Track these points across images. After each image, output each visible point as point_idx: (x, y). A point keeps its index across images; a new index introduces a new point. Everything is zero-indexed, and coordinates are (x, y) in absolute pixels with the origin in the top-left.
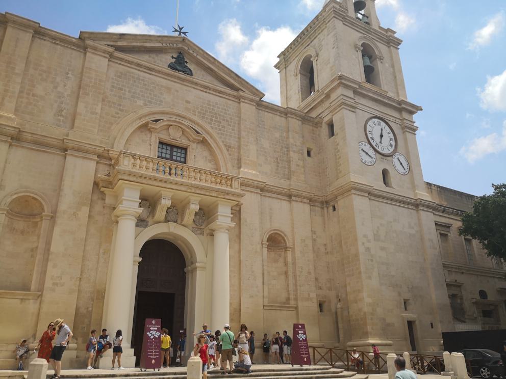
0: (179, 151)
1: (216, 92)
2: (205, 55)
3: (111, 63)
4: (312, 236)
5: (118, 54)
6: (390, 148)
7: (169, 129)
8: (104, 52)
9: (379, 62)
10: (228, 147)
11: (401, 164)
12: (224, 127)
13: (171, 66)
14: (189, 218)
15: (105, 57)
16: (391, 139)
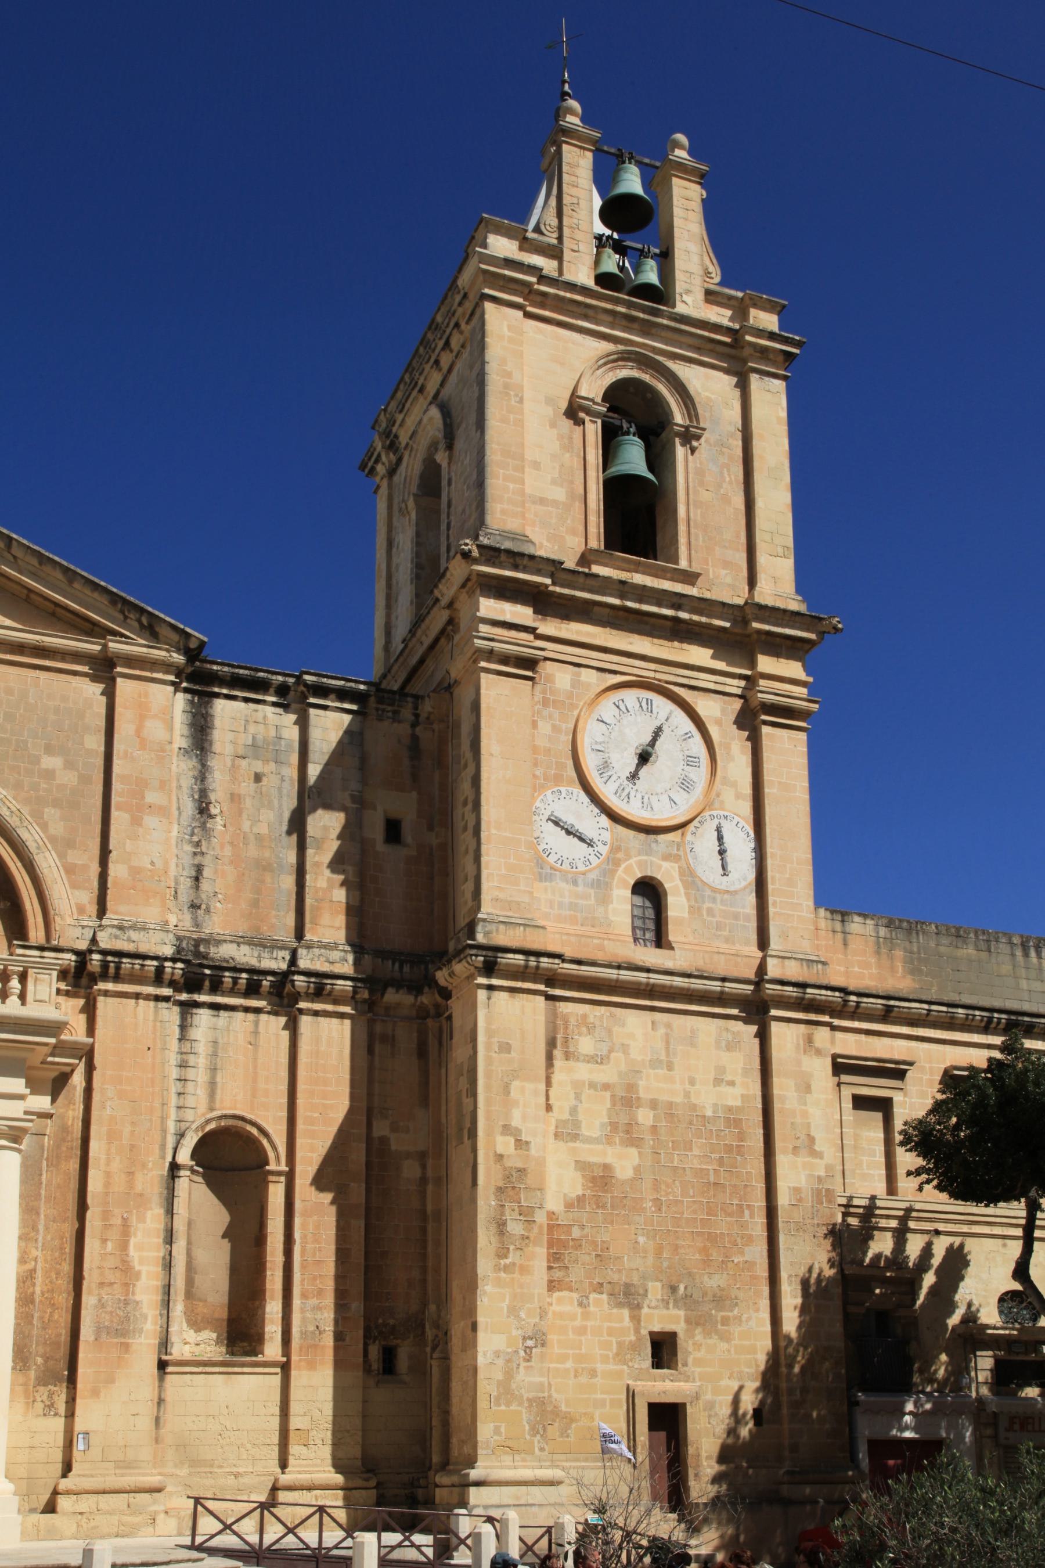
1: (22, 654)
6: (680, 796)
9: (680, 451)
10: (63, 845)
11: (722, 852)
16: (691, 761)
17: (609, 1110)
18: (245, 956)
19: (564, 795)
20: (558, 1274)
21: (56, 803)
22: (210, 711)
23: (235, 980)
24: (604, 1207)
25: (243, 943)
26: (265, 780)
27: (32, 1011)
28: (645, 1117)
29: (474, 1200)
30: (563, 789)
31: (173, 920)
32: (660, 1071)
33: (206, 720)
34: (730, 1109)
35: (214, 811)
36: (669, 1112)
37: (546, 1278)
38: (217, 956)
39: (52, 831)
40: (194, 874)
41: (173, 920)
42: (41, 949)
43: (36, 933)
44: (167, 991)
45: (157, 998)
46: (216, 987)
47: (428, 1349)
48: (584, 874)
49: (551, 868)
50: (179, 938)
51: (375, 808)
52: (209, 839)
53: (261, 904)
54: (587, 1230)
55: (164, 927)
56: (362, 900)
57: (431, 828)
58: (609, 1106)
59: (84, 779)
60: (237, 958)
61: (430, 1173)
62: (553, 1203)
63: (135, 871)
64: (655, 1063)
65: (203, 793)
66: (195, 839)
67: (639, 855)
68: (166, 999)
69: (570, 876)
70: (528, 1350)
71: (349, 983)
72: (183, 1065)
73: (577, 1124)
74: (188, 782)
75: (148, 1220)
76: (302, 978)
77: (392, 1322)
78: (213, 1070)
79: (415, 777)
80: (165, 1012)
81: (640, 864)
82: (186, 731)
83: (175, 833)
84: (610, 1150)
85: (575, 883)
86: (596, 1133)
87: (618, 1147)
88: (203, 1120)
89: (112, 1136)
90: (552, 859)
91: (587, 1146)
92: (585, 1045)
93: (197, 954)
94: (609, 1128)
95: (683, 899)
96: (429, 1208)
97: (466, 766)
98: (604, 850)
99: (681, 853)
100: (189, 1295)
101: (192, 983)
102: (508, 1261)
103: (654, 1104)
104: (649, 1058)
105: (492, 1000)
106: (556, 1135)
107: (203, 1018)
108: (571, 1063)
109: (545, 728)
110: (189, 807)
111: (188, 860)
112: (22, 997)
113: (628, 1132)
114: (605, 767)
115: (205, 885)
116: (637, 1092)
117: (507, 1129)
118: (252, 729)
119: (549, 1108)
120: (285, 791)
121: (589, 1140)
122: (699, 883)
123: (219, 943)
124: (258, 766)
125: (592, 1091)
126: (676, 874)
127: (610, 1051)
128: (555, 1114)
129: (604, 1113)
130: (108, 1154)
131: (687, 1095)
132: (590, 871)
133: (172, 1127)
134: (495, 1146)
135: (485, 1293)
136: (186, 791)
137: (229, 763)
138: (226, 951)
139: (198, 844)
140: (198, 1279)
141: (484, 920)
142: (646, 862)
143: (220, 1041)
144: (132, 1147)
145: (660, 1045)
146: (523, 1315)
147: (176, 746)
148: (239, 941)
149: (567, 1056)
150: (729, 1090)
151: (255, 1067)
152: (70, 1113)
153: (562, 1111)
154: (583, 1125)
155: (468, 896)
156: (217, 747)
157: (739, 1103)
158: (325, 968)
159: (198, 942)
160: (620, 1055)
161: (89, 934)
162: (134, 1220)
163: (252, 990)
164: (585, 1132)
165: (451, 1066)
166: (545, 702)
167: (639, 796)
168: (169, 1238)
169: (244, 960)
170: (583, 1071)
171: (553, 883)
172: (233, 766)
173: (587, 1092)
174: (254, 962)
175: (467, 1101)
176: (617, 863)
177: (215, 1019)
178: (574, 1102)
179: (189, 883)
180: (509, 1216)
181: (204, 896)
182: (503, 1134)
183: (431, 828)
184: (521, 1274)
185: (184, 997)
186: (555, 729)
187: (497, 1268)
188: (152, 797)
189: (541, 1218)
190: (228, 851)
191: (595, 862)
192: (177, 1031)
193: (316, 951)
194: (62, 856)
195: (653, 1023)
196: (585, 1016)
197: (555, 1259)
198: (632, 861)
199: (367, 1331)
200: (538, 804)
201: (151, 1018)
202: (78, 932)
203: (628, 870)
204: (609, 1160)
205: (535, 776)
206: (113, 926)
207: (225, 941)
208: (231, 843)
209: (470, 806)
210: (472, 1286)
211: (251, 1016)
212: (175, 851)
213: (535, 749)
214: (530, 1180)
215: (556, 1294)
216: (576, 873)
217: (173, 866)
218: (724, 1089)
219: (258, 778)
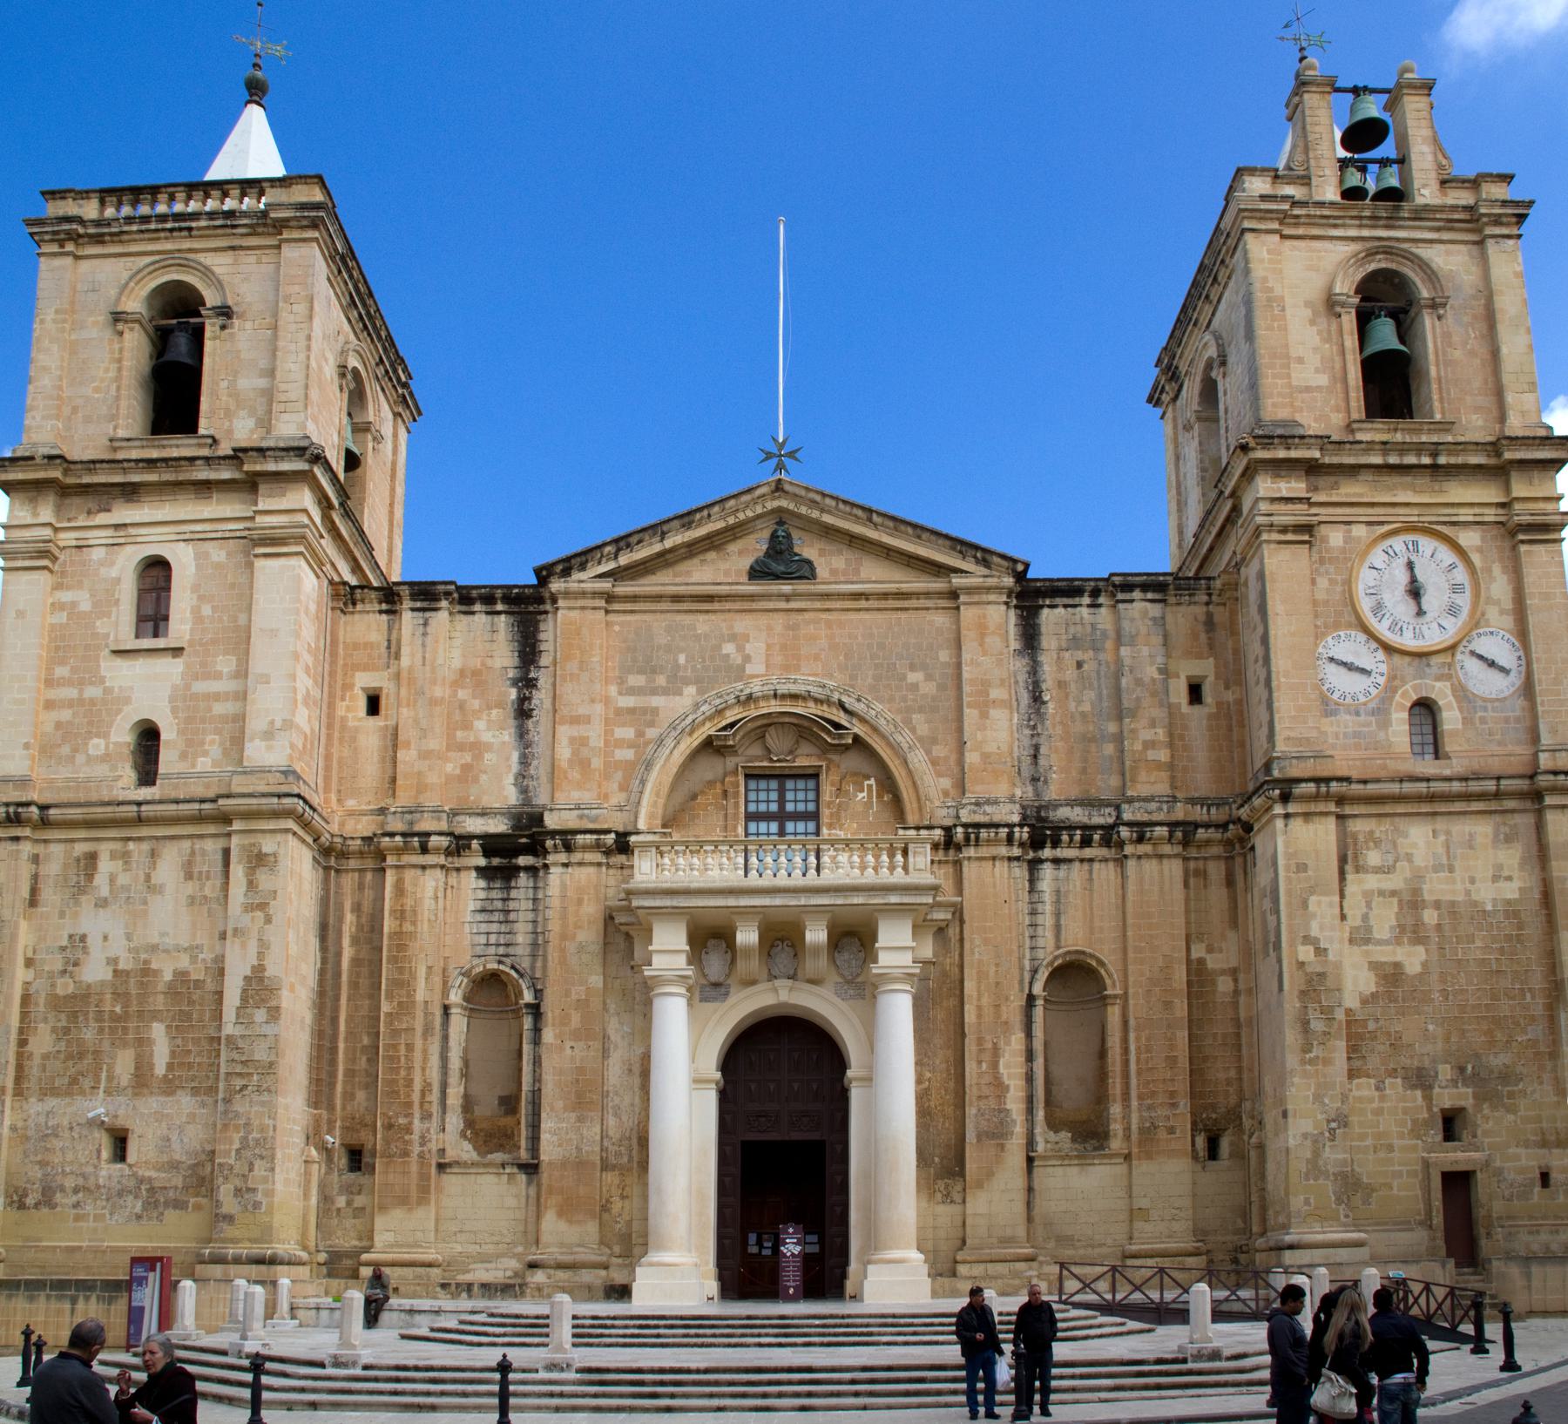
0: (801, 784)
2: (841, 506)
3: (612, 617)
4: (1188, 950)
7: (764, 737)
8: (596, 594)
10: (928, 743)
12: (914, 687)
13: (757, 573)
14: (817, 964)
15: (594, 608)
18: (1077, 815)
20: (1357, 1064)
21: (921, 710)
23: (1071, 837)
24: (1396, 1001)
26: (1086, 667)
27: (914, 878)
29: (1280, 1004)
31: (1018, 793)
34: (1509, 902)
35: (1046, 698)
36: (1451, 910)
37: (1346, 1067)
38: (1055, 819)
39: (919, 732)
40: (1032, 752)
41: (1018, 793)
42: (918, 828)
43: (912, 819)
44: (1016, 852)
45: (1010, 859)
46: (1056, 843)
47: (1246, 1138)
49: (1337, 704)
50: (1023, 807)
51: (1178, 677)
52: (1043, 724)
53: (1089, 771)
54: (1381, 1023)
55: (1012, 800)
56: (1172, 756)
57: (1227, 687)
58: (1396, 910)
59: (942, 687)
61: (1241, 986)
62: (1351, 1001)
63: (985, 757)
66: (1032, 723)
68: (1018, 859)
70: (1332, 1131)
71: (1165, 828)
72: (1033, 913)
74: (1022, 677)
75: (1013, 1043)
76: (1125, 828)
77: (1214, 1116)
78: (1057, 915)
79: (1211, 646)
80: (1017, 870)
83: (1015, 721)
88: (1051, 957)
89: (981, 975)
92: (1373, 858)
93: (1040, 819)
96: (1242, 1015)
97: (1255, 629)
100: (1048, 1103)
101: (1036, 843)
102: (1312, 1055)
105: (1289, 827)
106: (1351, 941)
107: (1047, 872)
109: (1323, 583)
110: (1025, 698)
111: (1027, 742)
112: (905, 868)
114: (1378, 608)
115: (1042, 761)
117: (1307, 940)
119: (1343, 917)
120: (1102, 673)
123: (1056, 807)
124: (1080, 655)
128: (1350, 922)
130: (979, 991)
131: (1468, 893)
133: (1027, 964)
134: (1297, 955)
135: (1293, 1084)
137: (1055, 656)
138: (1063, 813)
139: (1034, 727)
140: (1055, 1089)
141: (1278, 758)
144: (997, 984)
146: (1327, 1101)
147: (1012, 648)
148: (1071, 803)
149: (1358, 869)
150: (1508, 884)
151: (1091, 909)
152: (948, 960)
153: (1354, 918)
155: (1264, 739)
157: (1516, 896)
158: (1146, 818)
159: (1039, 808)
161: (952, 812)
162: (1002, 1044)
163: (1086, 842)
165: (1256, 890)
168: (1030, 1056)
169: (1078, 819)
170: (1372, 882)
173: (1376, 900)
174: (1085, 820)
175: (1271, 919)
177: (1056, 872)
178: (1365, 910)
179: (1029, 760)
180: (1312, 1015)
182: (1304, 944)
183: (1227, 687)
184: (1324, 1065)
185: (1031, 855)
187: (1303, 1062)
188: (996, 693)
189: (1340, 1015)
190: (1059, 730)
192: (1027, 884)
193: (1136, 804)
194: (928, 752)
197: (1353, 1050)
199: (1194, 1124)
200: (1320, 650)
202: (944, 812)
205: (1316, 626)
206: (971, 804)
208: (1061, 723)
209: (1261, 662)
210: (1281, 1081)
211: (1086, 866)
212: (1016, 735)
213: (1315, 603)
214: (1329, 983)
215: (1356, 1081)
217: (1016, 749)
218: (1502, 884)
219: (1079, 665)
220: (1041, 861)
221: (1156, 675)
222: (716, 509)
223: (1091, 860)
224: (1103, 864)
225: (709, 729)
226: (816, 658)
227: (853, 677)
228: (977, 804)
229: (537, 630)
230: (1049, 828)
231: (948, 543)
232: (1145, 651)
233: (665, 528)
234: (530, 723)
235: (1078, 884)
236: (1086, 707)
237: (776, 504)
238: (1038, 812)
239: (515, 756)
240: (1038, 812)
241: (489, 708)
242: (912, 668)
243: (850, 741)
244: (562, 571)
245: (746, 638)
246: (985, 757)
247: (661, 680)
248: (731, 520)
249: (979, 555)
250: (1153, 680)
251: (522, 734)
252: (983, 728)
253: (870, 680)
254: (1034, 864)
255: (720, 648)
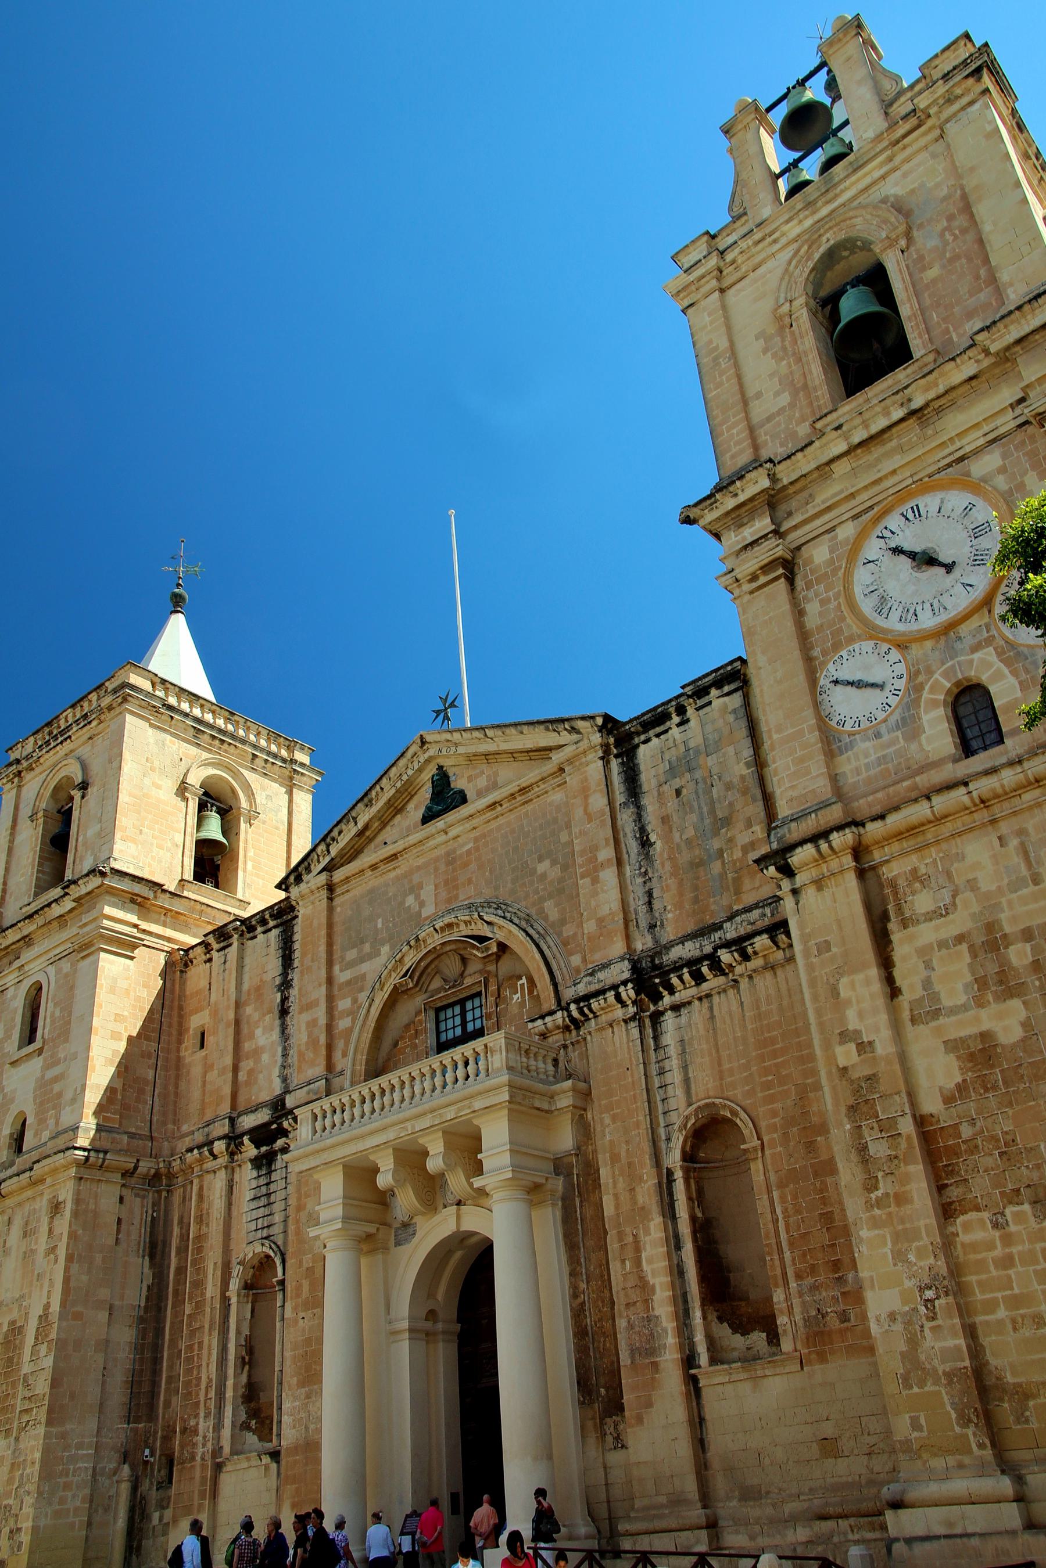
5: (339, 875)
12: (544, 876)
17: (970, 965)
18: (689, 950)
19: (845, 657)
21: (550, 896)
22: (636, 762)
23: (680, 978)
25: (687, 941)
26: (684, 791)
28: (1019, 955)
30: (844, 653)
32: (1025, 891)
33: (634, 771)
35: (653, 838)
40: (647, 899)
48: (885, 721)
53: (701, 897)
60: (684, 956)
63: (600, 921)
64: (1015, 886)
65: (642, 830)
66: (643, 870)
67: (943, 664)
69: (870, 732)
71: (765, 936)
73: (935, 997)
81: (946, 675)
82: (622, 789)
84: (983, 1013)
85: (878, 735)
86: (962, 999)
87: (993, 1005)
90: (848, 727)
91: (953, 1018)
94: (976, 986)
95: (1012, 680)
98: (901, 684)
99: (994, 632)
103: (1027, 935)
104: (1006, 881)
108: (911, 930)
113: (1001, 982)
115: (657, 905)
116: (1001, 929)
118: (667, 757)
120: (700, 791)
121: (953, 1011)
122: (1025, 650)
124: (677, 783)
125: (944, 951)
126: (994, 658)
127: (954, 897)
129: (966, 971)
132: (891, 713)
136: (630, 835)
139: (646, 873)
142: (953, 666)
143: (686, 1038)
145: (1017, 860)
148: (682, 940)
154: (942, 996)
156: (645, 787)
160: (969, 895)
164: (947, 1002)
166: (809, 585)
167: (927, 606)
171: (855, 749)
172: (659, 794)
176: (919, 689)
179: (645, 908)
181: (657, 915)
186: (824, 602)
190: (668, 866)
191: (893, 701)
193: (738, 919)
195: (1000, 838)
196: (915, 870)
198: (937, 676)
201: (625, 1040)
203: (932, 690)
204: (985, 1027)
207: (673, 946)
208: (670, 858)
211: (706, 1003)
216: (878, 724)
219: (678, 793)
220: (662, 1013)
221: (745, 771)
222: (384, 781)
223: (708, 996)
224: (723, 995)
225: (394, 980)
226: (470, 881)
227: (496, 888)
228: (591, 974)
229: (292, 934)
230: (656, 977)
231: (542, 727)
232: (730, 750)
233: (354, 814)
234: (288, 1019)
235: (701, 1026)
236: (690, 832)
237: (426, 756)
238: (653, 961)
239: (280, 1049)
240: (653, 961)
241: (264, 1015)
242: (541, 859)
243: (494, 949)
244: (295, 879)
245: (420, 886)
246: (600, 921)
247: (367, 948)
248: (399, 785)
249: (567, 726)
250: (743, 777)
251: (284, 1028)
252: (595, 894)
253: (509, 885)
254: (656, 1018)
255: (403, 902)
